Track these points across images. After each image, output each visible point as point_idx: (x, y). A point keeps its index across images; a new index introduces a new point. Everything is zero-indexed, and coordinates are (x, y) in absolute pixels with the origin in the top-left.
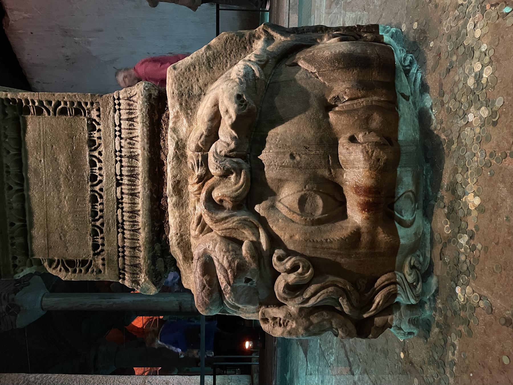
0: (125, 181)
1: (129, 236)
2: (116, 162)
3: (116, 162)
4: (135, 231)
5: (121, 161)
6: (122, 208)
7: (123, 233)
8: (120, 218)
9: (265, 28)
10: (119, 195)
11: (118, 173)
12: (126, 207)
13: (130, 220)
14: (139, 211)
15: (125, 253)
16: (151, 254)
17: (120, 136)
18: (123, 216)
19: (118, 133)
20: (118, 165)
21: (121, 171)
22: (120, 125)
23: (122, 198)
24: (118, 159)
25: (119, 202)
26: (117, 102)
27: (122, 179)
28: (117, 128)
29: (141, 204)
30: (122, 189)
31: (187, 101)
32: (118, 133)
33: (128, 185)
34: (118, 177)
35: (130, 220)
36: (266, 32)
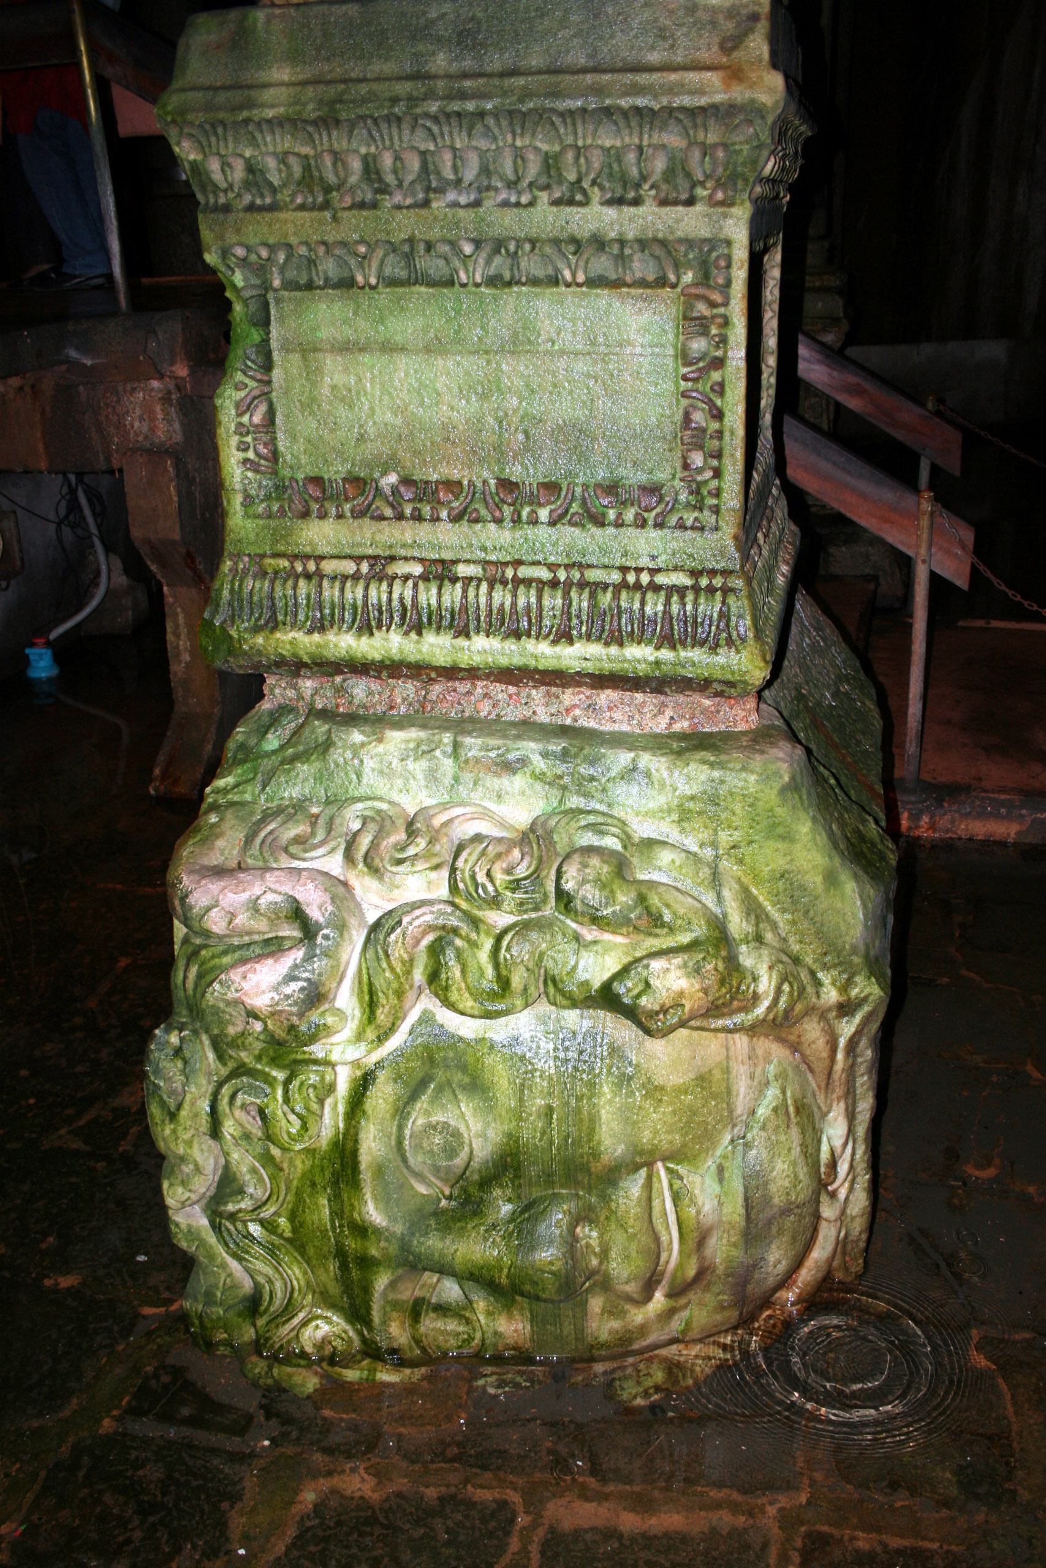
0: (502, 597)
1: (349, 595)
2: (552, 567)
3: (552, 567)
4: (367, 623)
5: (554, 584)
6: (425, 578)
7: (356, 577)
8: (401, 568)
9: (871, 998)
10: (462, 570)
11: (524, 572)
12: (428, 596)
13: (395, 603)
14: (420, 634)
15: (302, 583)
16: (306, 659)
17: (624, 584)
18: (406, 578)
19: (631, 578)
20: (545, 574)
21: (528, 582)
22: (656, 588)
23: (454, 580)
24: (562, 575)
25: (440, 572)
26: (718, 582)
27: (504, 582)
28: (645, 578)
29: (436, 647)
30: (480, 580)
31: (700, 813)
32: (631, 578)
33: (490, 605)
34: (509, 573)
35: (395, 603)
36: (865, 999)
